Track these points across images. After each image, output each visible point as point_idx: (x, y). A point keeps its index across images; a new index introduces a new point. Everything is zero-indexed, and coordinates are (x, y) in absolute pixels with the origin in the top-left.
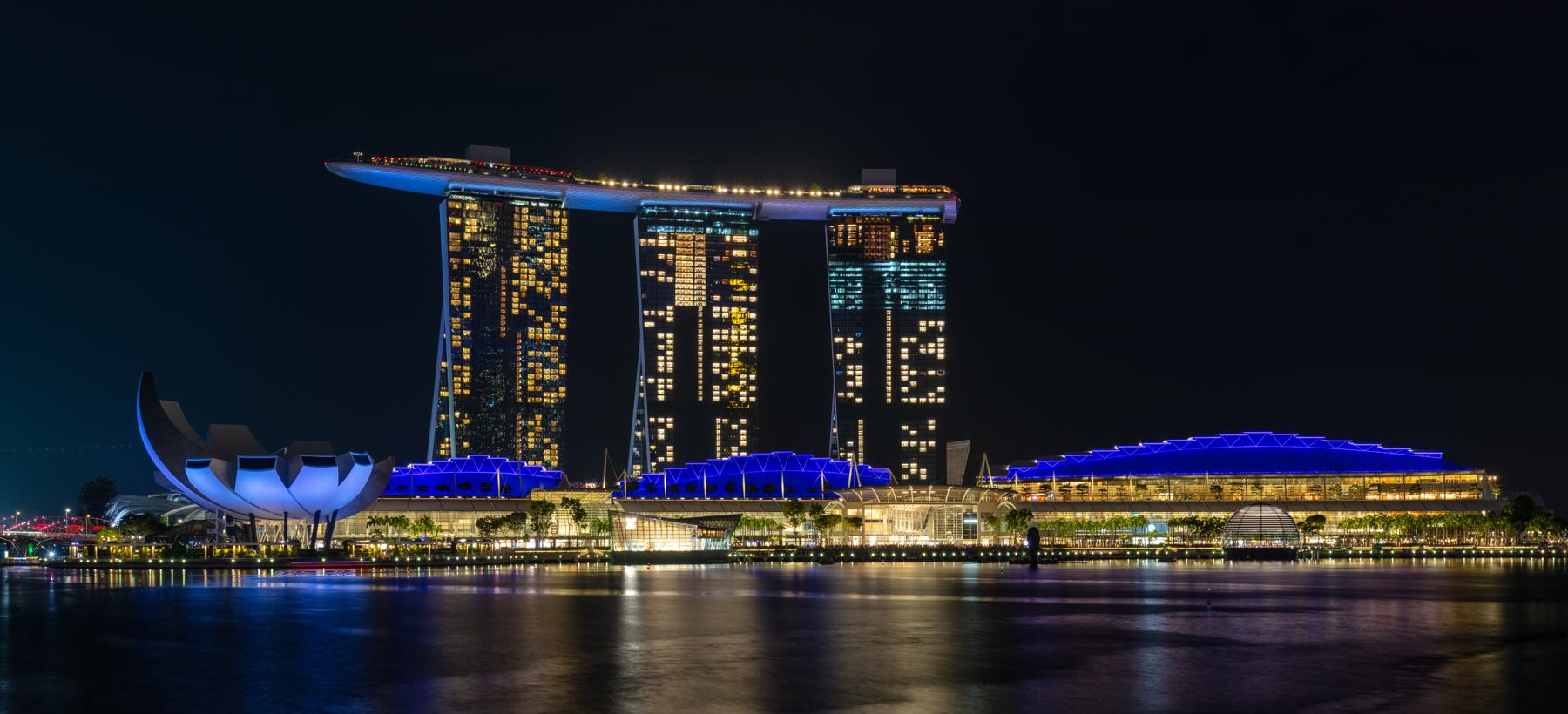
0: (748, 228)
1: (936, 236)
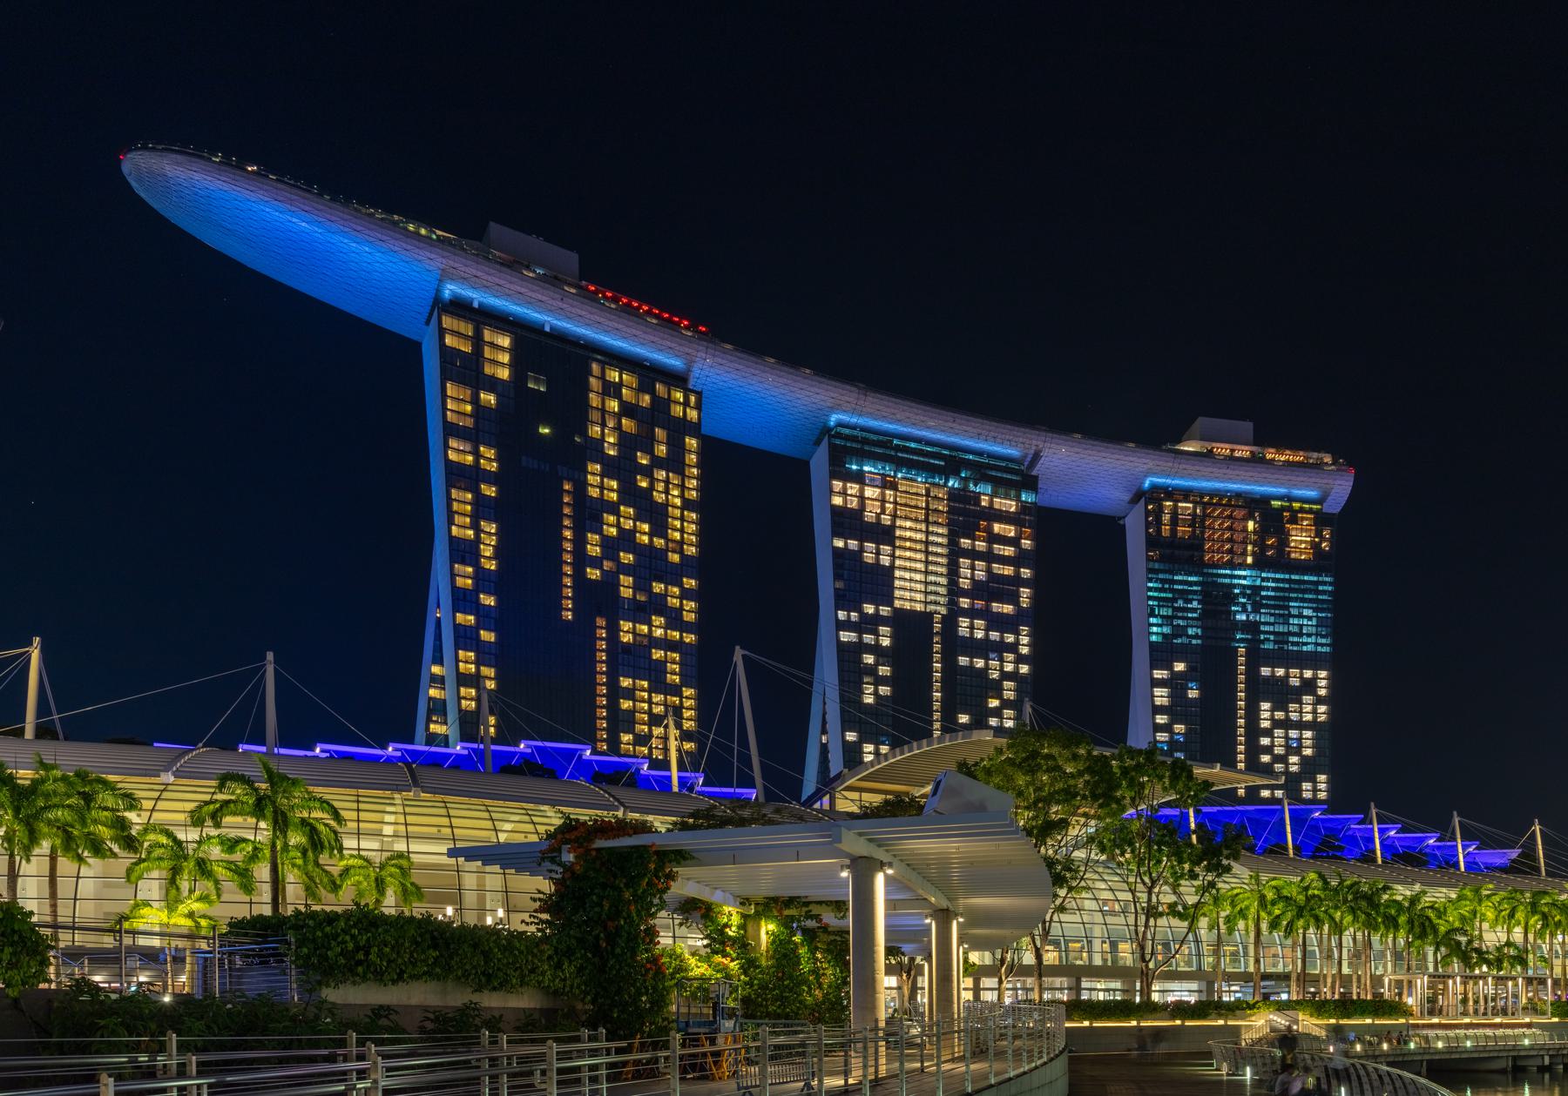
1: (1319, 534)
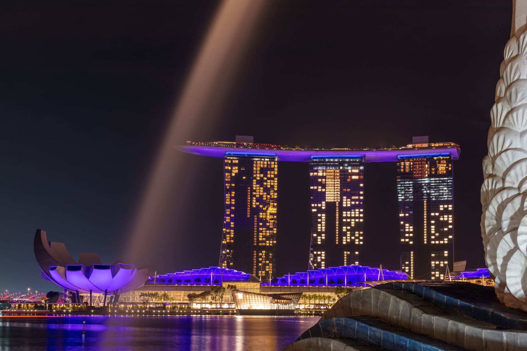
0: (359, 166)
1: (448, 166)
